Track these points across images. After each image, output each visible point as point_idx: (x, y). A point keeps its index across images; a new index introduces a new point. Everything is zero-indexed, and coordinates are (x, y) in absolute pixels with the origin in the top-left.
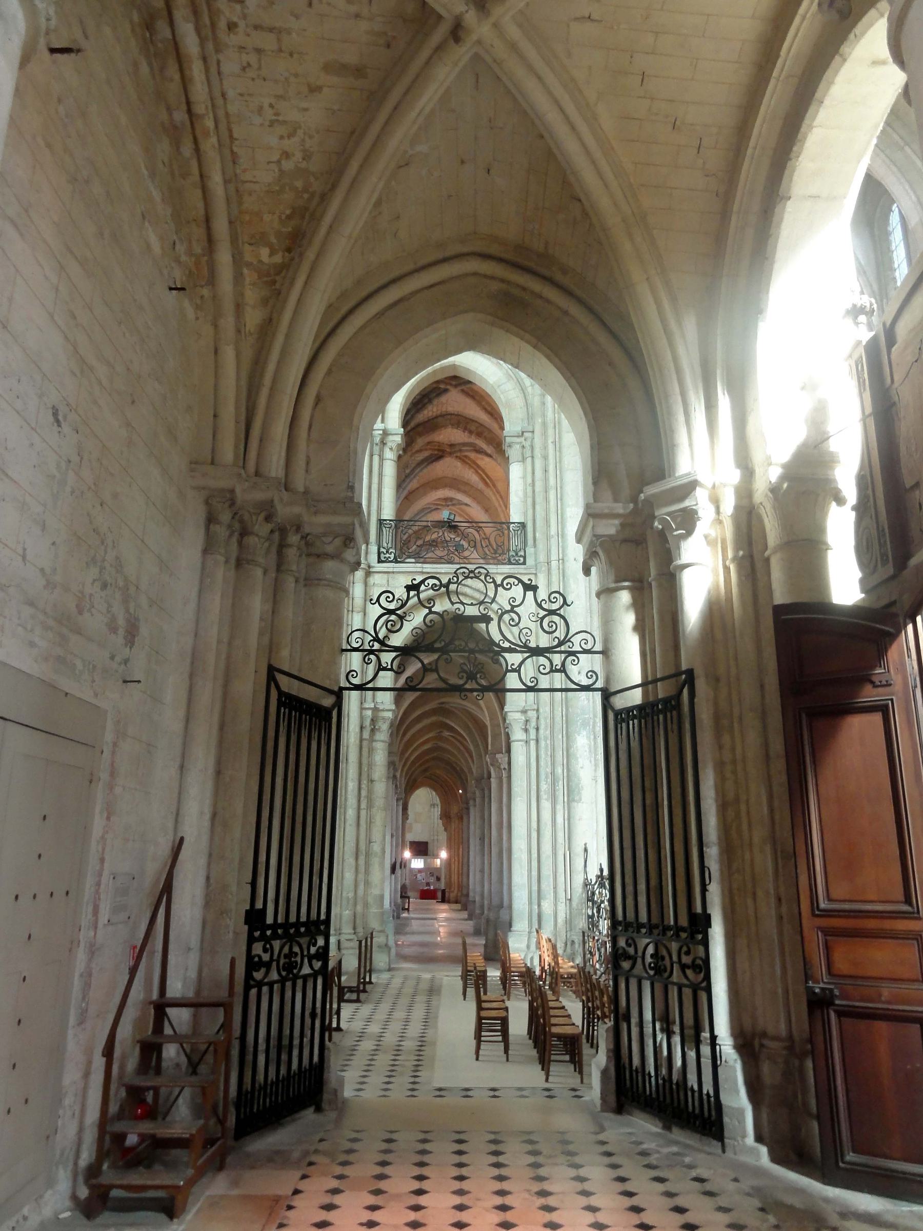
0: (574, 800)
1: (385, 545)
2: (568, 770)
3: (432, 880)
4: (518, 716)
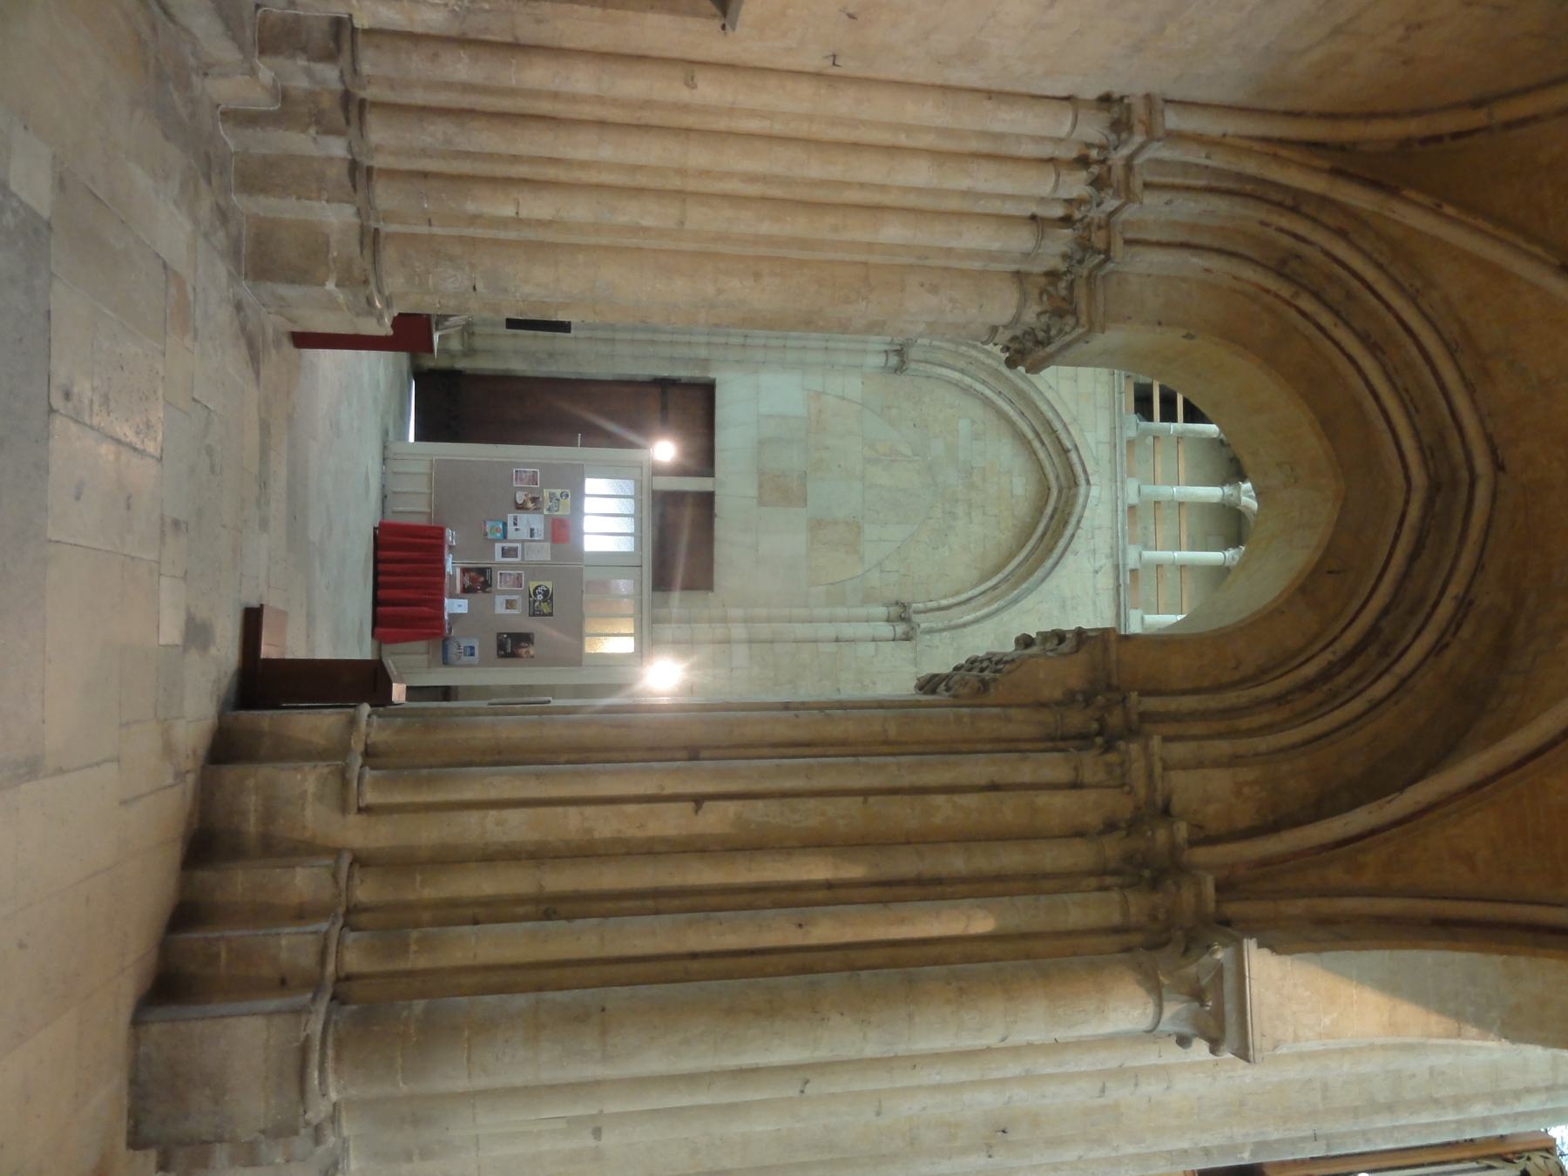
3: (504, 608)
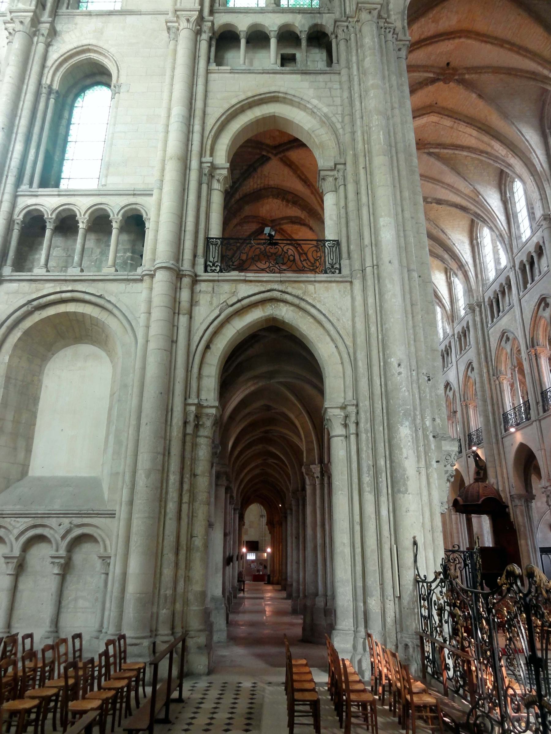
0: (399, 491)
1: (211, 259)
2: (392, 461)
3: (261, 568)
4: (337, 412)
